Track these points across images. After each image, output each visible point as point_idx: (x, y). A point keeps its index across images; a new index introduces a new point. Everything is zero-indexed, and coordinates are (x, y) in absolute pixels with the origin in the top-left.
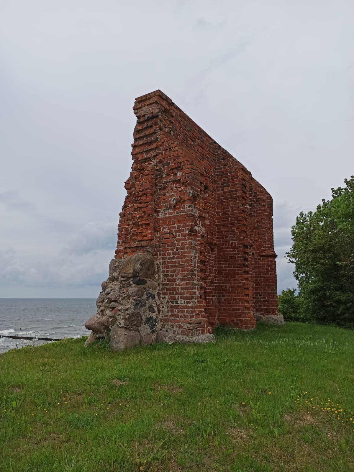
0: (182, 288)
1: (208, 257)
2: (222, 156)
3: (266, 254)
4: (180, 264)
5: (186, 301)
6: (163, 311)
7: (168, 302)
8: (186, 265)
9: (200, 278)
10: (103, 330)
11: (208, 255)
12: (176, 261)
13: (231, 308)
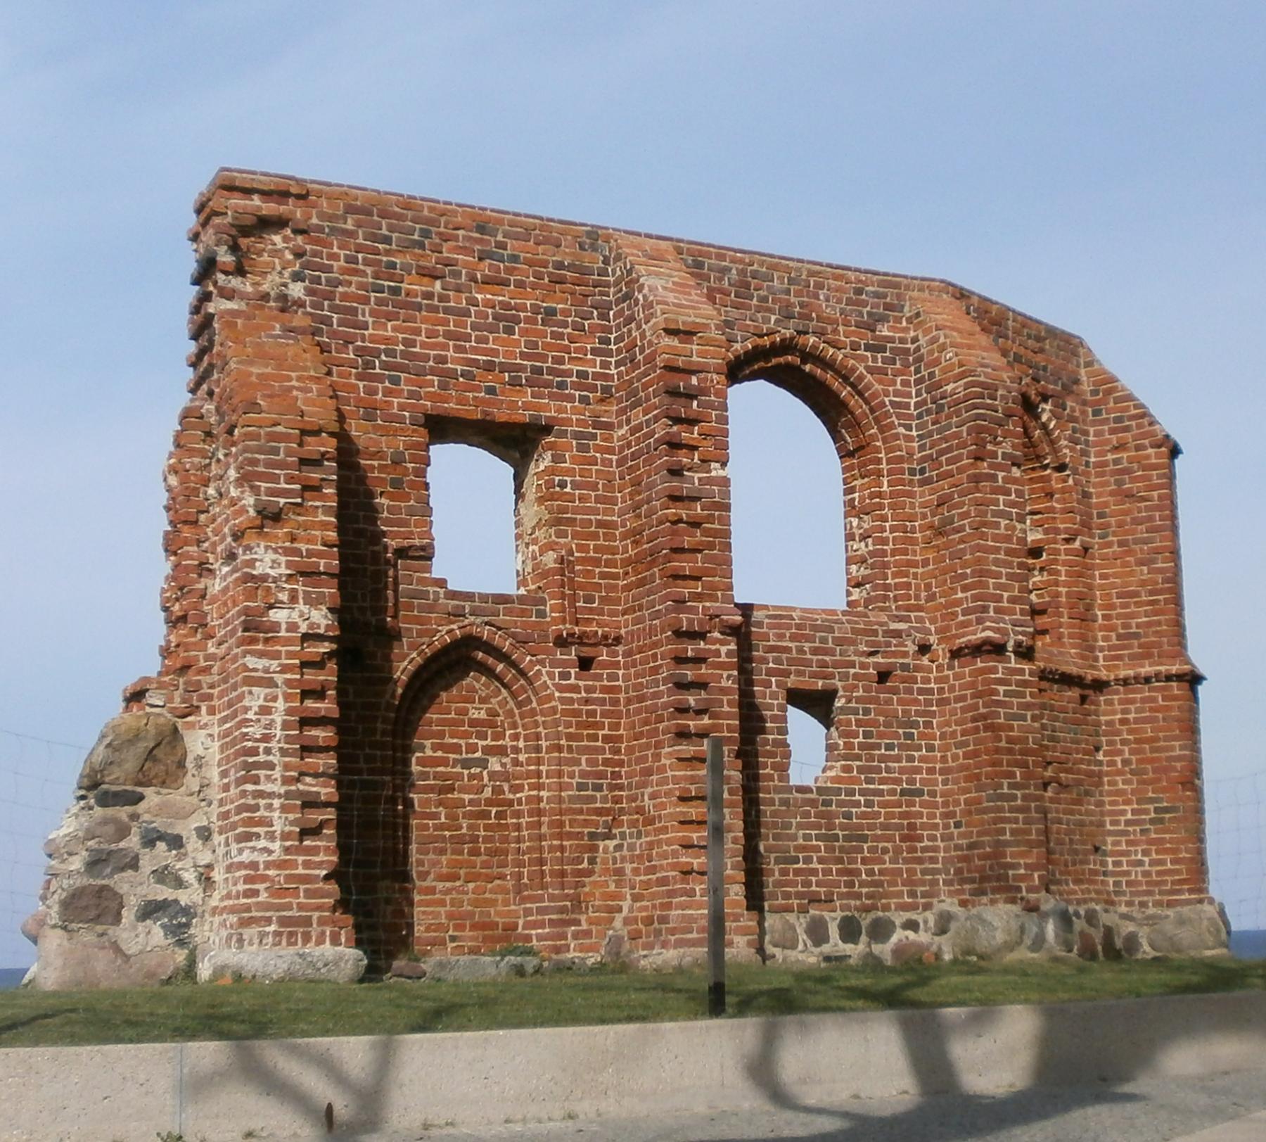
11: (553, 684)
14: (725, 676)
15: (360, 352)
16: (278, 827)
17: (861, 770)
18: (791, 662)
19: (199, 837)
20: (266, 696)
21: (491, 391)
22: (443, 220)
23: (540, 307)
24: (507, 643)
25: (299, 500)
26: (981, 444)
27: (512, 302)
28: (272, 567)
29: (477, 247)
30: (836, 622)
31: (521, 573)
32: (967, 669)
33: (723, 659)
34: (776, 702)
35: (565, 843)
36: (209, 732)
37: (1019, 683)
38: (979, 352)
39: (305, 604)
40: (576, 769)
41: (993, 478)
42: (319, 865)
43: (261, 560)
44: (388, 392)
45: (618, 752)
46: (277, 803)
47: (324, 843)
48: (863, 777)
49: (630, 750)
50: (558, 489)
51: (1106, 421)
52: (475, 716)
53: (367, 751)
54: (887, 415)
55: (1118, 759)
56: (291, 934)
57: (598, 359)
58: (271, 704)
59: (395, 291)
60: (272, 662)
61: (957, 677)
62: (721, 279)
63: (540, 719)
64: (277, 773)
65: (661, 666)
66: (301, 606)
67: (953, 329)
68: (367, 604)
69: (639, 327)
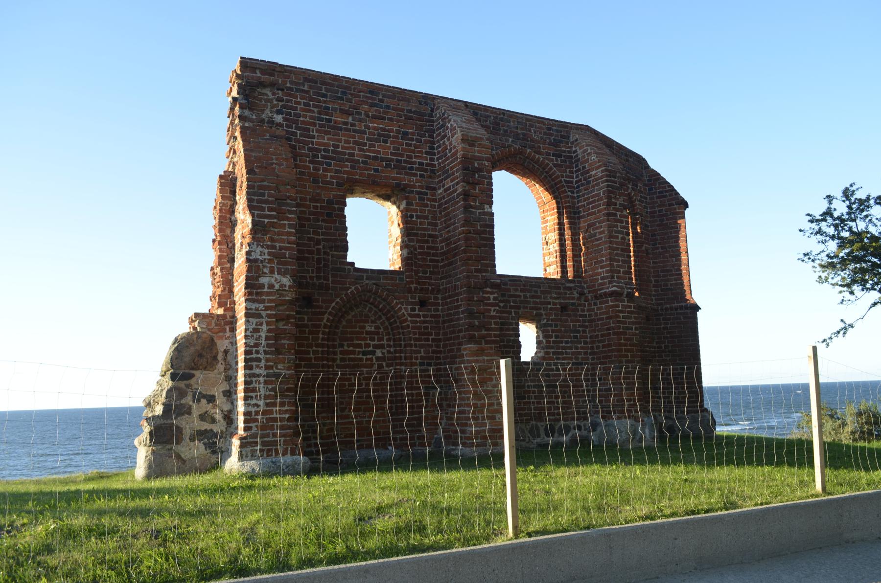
1: (411, 317)
11: (408, 314)
14: (492, 309)
15: (310, 149)
16: (263, 392)
17: (554, 353)
18: (521, 302)
19: (224, 396)
20: (257, 323)
21: (376, 170)
22: (353, 87)
23: (400, 131)
24: (385, 294)
25: (275, 220)
26: (609, 198)
27: (387, 128)
28: (260, 255)
29: (370, 101)
30: (541, 283)
31: (392, 260)
32: (604, 306)
33: (492, 301)
34: (514, 321)
35: (413, 392)
36: (231, 341)
37: (629, 312)
38: (607, 157)
39: (278, 274)
40: (419, 355)
41: (616, 215)
42: (286, 412)
43: (255, 251)
44: (325, 170)
45: (438, 346)
46: (262, 379)
47: (288, 400)
48: (555, 357)
49: (445, 346)
50: (409, 219)
51: (655, 193)
52: (370, 330)
53: (314, 348)
54: (563, 186)
55: (663, 346)
56: (269, 451)
57: (429, 157)
58: (259, 327)
59: (329, 121)
60: (260, 305)
62: (486, 121)
63: (401, 331)
64: (262, 364)
65: (461, 305)
66: (276, 275)
67: (593, 146)
68: (314, 275)
69: (448, 140)
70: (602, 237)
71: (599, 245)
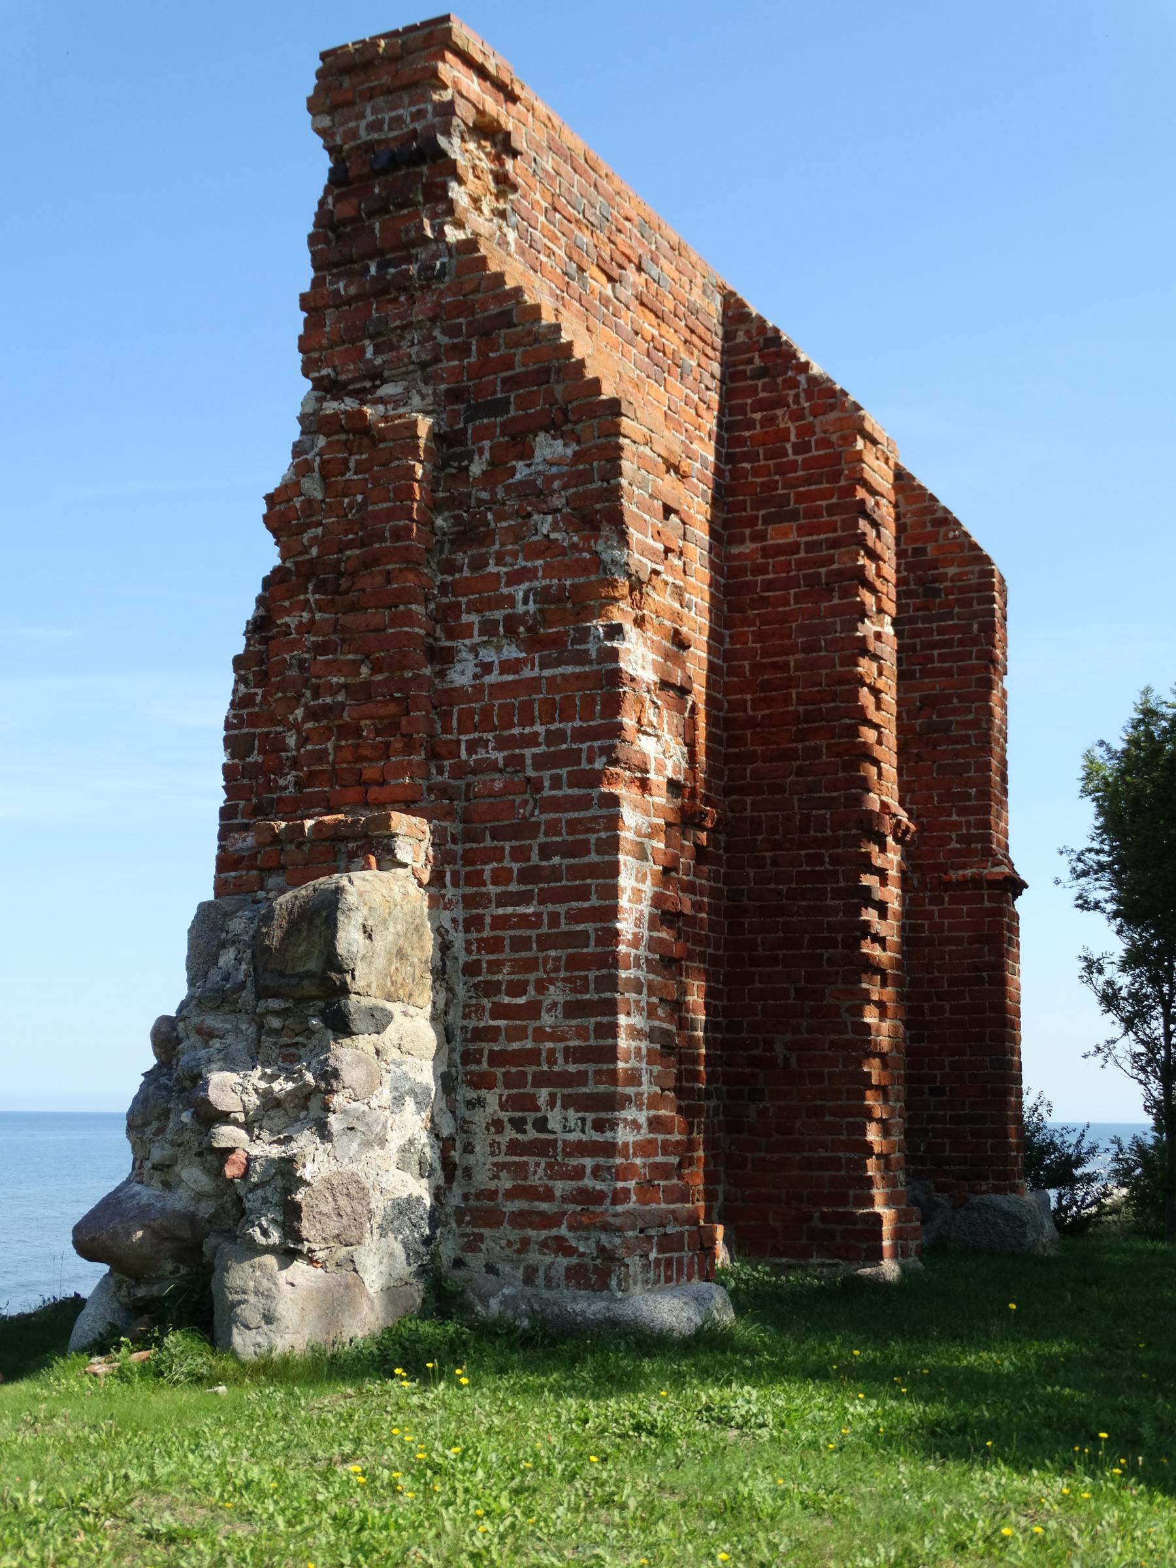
0: (571, 1054)
2: (757, 360)
3: (969, 872)
4: (564, 928)
5: (590, 1116)
6: (468, 1172)
7: (498, 1125)
8: (593, 937)
9: (661, 1000)
10: (169, 1266)
12: (538, 915)
13: (798, 1157)
36: (454, 914)
61: (943, 913)
65: (836, 872)
69: (797, 416)
70: (968, 737)
71: (957, 754)
